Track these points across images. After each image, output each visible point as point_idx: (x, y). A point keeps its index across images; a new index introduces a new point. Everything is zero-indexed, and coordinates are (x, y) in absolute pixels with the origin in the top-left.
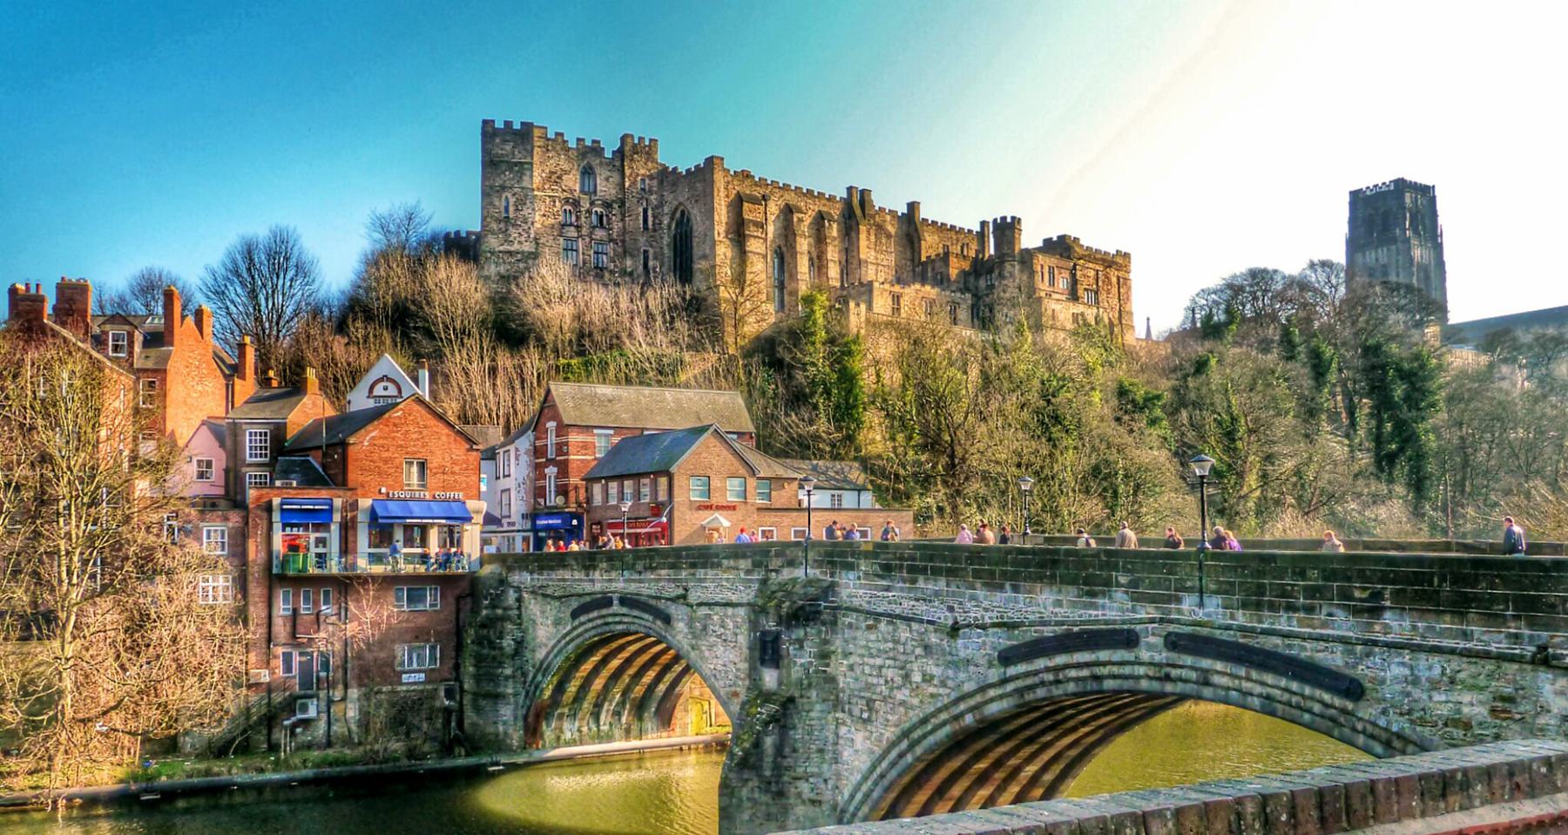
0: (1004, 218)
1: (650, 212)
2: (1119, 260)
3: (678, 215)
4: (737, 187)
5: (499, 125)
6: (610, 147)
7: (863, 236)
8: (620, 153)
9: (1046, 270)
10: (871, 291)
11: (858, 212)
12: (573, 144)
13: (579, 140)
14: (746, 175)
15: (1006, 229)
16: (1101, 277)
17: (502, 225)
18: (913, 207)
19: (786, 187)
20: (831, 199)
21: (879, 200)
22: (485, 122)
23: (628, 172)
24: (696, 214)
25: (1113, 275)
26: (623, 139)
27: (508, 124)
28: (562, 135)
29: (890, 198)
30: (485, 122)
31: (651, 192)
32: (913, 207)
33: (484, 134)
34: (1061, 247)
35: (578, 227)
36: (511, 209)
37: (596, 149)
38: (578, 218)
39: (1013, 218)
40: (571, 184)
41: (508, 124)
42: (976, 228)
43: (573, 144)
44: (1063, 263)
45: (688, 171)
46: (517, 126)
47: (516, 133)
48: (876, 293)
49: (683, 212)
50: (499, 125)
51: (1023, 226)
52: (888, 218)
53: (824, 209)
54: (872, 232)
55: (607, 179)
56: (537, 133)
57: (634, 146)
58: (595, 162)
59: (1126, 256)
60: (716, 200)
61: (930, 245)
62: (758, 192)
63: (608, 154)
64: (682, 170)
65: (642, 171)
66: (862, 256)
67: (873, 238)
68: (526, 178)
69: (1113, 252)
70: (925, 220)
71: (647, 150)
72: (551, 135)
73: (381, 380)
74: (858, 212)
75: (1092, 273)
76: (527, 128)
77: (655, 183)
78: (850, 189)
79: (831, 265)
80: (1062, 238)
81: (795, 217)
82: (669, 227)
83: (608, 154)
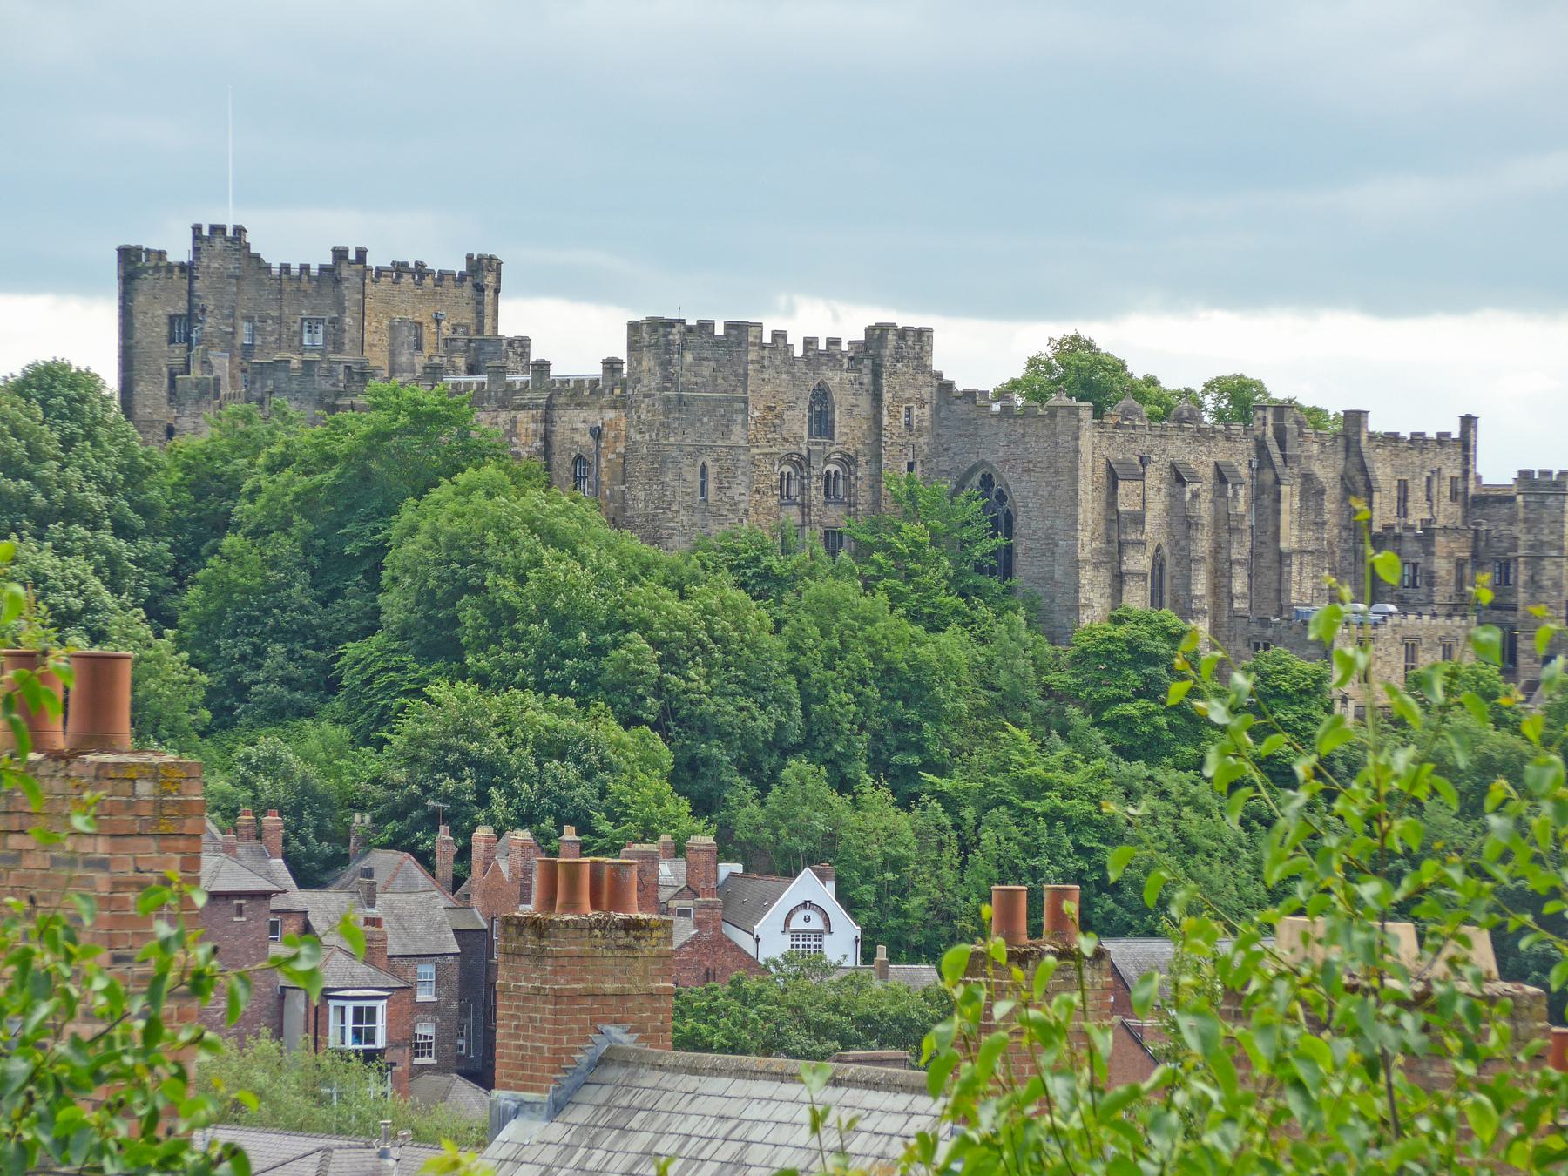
17: (697, 518)
23: (887, 396)
24: (1022, 492)
47: (718, 342)
53: (1221, 458)
65: (908, 393)
73: (806, 905)
77: (927, 410)
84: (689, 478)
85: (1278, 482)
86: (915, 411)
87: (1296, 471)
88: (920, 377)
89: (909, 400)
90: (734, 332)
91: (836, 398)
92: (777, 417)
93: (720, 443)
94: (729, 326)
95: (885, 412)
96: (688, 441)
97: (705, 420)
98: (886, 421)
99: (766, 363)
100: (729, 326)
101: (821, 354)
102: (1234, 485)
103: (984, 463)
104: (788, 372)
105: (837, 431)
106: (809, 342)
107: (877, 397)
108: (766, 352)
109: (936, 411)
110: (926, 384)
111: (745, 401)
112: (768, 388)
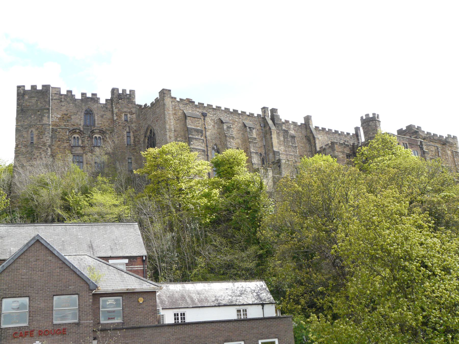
0: (367, 115)
1: (131, 134)
2: (451, 141)
3: (148, 133)
5: (28, 88)
6: (104, 96)
7: (274, 136)
8: (110, 102)
10: (280, 166)
11: (270, 122)
13: (83, 94)
14: (190, 102)
15: (370, 123)
18: (308, 119)
20: (251, 115)
21: (283, 116)
22: (19, 87)
23: (115, 111)
24: (157, 129)
26: (114, 91)
27: (34, 87)
28: (71, 92)
30: (19, 87)
31: (131, 122)
32: (308, 119)
33: (18, 94)
35: (83, 147)
36: (35, 138)
38: (83, 142)
39: (374, 114)
40: (78, 121)
41: (34, 87)
42: (352, 132)
46: (39, 88)
48: (283, 167)
49: (151, 131)
50: (28, 88)
51: (380, 119)
52: (292, 126)
54: (281, 134)
55: (102, 116)
57: (119, 95)
58: (94, 107)
59: (455, 138)
61: (321, 141)
62: (197, 113)
63: (103, 101)
64: (149, 104)
65: (125, 110)
68: (45, 119)
69: (445, 135)
70: (317, 128)
74: (270, 122)
75: (433, 149)
76: (46, 88)
77: (134, 116)
78: (264, 109)
80: (410, 128)
82: (144, 142)
83: (103, 101)
84: (26, 136)
86: (129, 115)
88: (130, 105)
89: (125, 112)
91: (95, 112)
93: (38, 123)
94: (43, 86)
95: (115, 115)
96: (26, 124)
97: (33, 116)
99: (63, 100)
100: (43, 86)
101: (89, 98)
103: (149, 126)
104: (72, 103)
105: (96, 122)
106: (83, 94)
107: (113, 112)
109: (138, 116)
110: (133, 107)
111: (49, 109)
112: (64, 108)
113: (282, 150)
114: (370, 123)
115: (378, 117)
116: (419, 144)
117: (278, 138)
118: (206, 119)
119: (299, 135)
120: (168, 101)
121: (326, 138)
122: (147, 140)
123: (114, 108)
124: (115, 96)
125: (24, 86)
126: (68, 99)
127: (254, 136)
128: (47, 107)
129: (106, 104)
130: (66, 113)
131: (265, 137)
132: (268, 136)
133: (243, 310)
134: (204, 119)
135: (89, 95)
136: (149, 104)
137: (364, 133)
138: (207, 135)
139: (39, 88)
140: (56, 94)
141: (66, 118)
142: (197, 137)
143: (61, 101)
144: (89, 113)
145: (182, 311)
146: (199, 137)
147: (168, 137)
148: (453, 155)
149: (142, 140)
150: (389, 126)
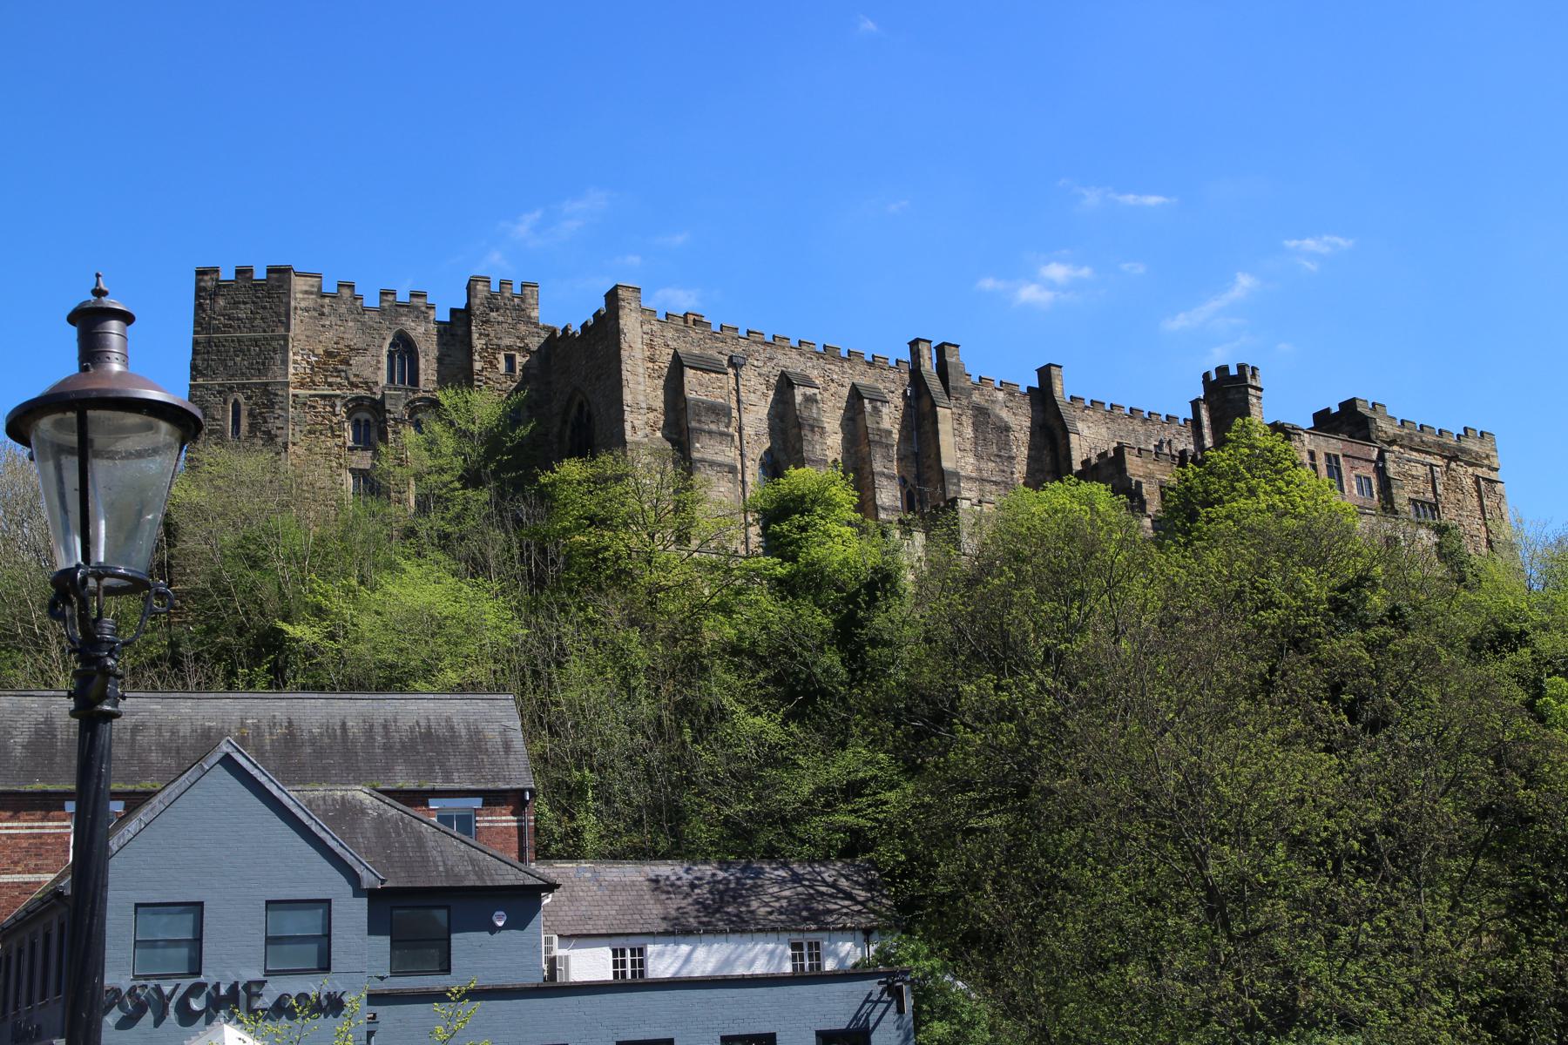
0: (1222, 370)
2: (1471, 444)
3: (574, 411)
4: (674, 341)
9: (1321, 462)
11: (935, 384)
12: (372, 300)
15: (1227, 393)
16: (1441, 480)
19: (776, 342)
21: (972, 362)
22: (201, 273)
23: (478, 343)
25: (1465, 474)
27: (244, 272)
28: (351, 287)
29: (997, 360)
30: (201, 273)
33: (199, 290)
34: (1347, 421)
37: (417, 305)
39: (1241, 367)
40: (367, 373)
43: (372, 300)
44: (1356, 449)
45: (584, 326)
46: (260, 274)
47: (257, 286)
49: (581, 405)
50: (227, 274)
53: (858, 380)
54: (967, 421)
56: (299, 285)
60: (626, 366)
61: (1088, 440)
64: (576, 328)
65: (507, 341)
66: (947, 464)
67: (969, 432)
71: (512, 302)
72: (330, 287)
74: (935, 384)
75: (1420, 471)
78: (914, 345)
79: (881, 482)
80: (1349, 406)
81: (799, 394)
85: (934, 405)
87: (965, 402)
88: (522, 327)
89: (509, 348)
90: (274, 275)
92: (341, 362)
94: (270, 271)
95: (476, 357)
98: (478, 366)
99: (326, 310)
100: (270, 271)
102: (871, 400)
104: (356, 320)
108: (327, 300)
110: (532, 334)
111: (286, 339)
113: (970, 468)
114: (1227, 393)
115: (1254, 376)
116: (1374, 456)
117: (958, 433)
118: (743, 372)
119: (1020, 422)
120: (630, 324)
121: (1104, 431)
122: (568, 432)
123: (475, 336)
124: (478, 301)
125: (216, 270)
126: (343, 309)
127: (886, 424)
128: (282, 331)
129: (451, 323)
130: (332, 347)
131: (919, 427)
132: (927, 427)
133: (810, 945)
134: (737, 376)
135: (403, 296)
136: (576, 328)
137: (1213, 420)
138: (744, 420)
139: (260, 274)
140: (306, 292)
141: (334, 361)
142: (713, 427)
143: (322, 314)
144: (404, 348)
145: (636, 942)
146: (723, 429)
147: (628, 426)
148: (1479, 491)
149: (555, 430)
150: (1286, 398)
